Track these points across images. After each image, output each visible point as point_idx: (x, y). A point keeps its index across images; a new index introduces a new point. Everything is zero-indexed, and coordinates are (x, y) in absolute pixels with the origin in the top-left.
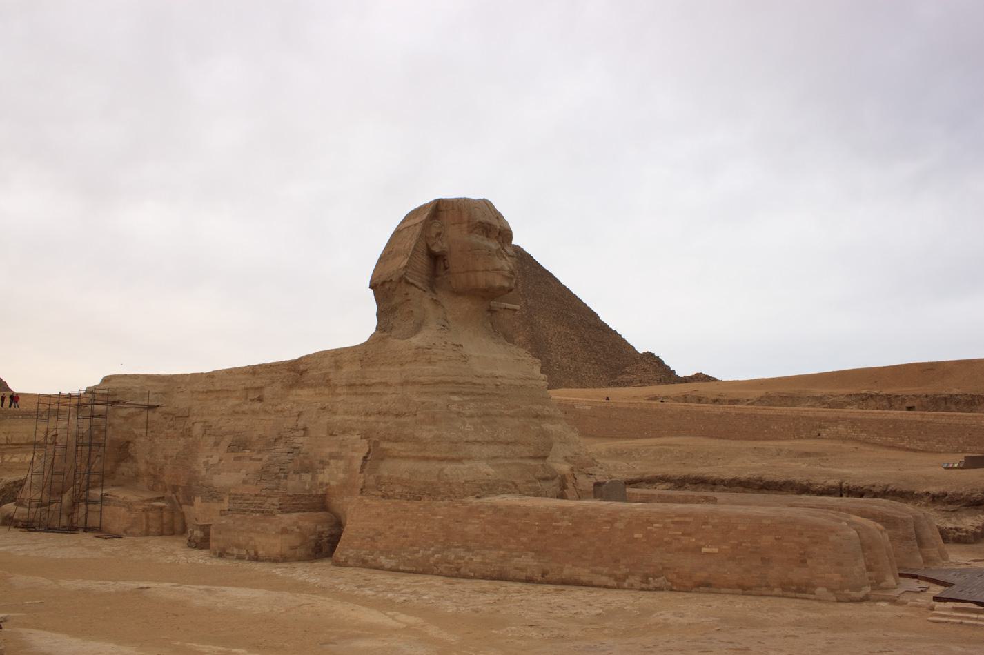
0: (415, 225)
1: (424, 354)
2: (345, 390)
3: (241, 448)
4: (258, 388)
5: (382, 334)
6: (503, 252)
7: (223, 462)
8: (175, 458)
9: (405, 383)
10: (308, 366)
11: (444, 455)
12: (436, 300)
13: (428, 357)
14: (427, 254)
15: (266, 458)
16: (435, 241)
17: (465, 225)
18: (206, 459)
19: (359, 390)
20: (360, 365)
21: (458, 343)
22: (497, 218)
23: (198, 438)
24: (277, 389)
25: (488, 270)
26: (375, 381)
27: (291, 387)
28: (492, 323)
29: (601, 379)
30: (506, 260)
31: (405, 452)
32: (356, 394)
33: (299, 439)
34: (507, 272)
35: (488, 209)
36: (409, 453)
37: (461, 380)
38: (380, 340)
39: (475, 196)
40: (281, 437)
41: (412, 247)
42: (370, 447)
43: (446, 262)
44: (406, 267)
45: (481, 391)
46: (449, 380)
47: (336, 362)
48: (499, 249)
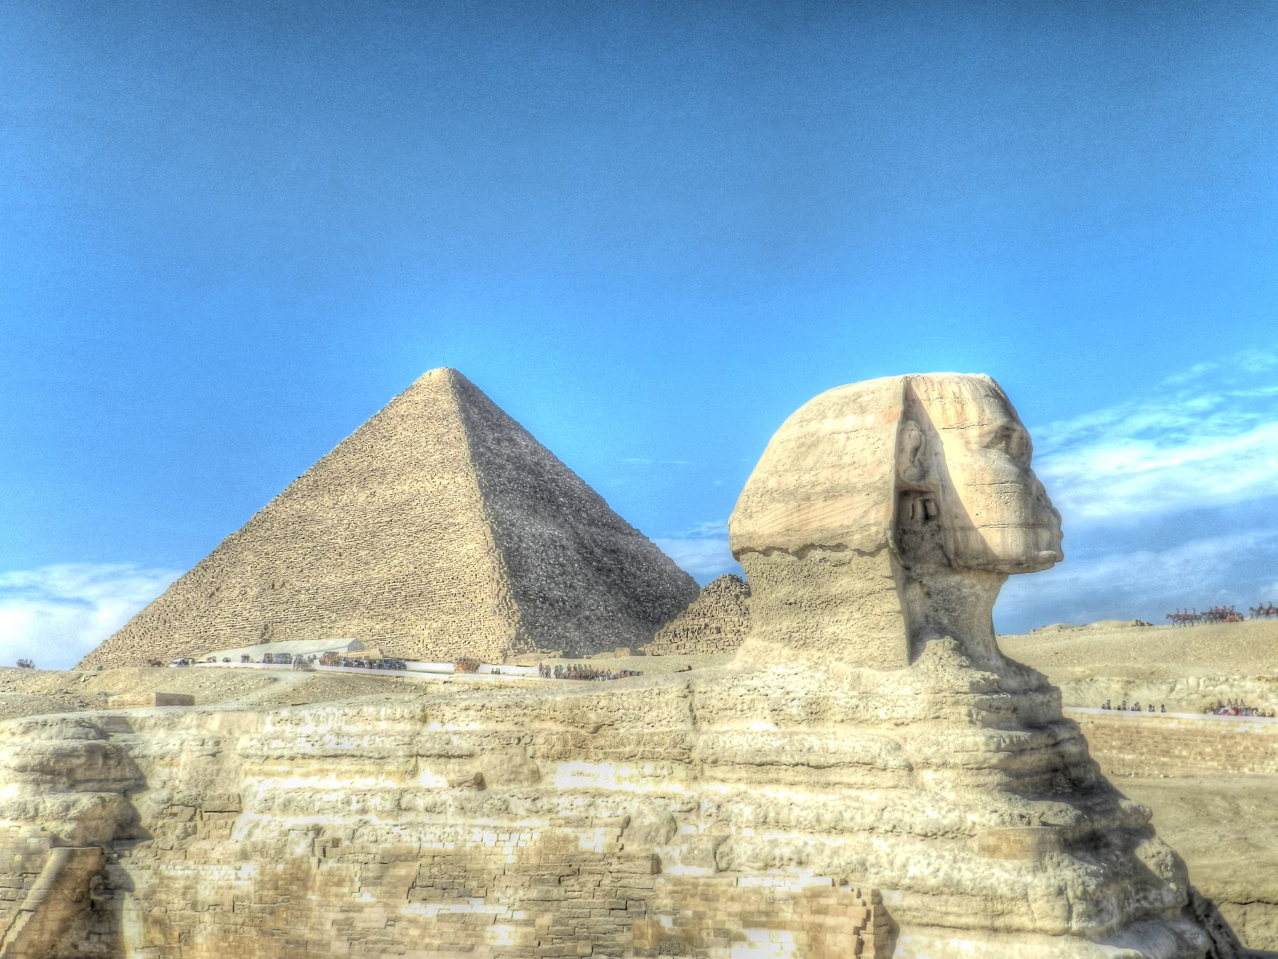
3: (455, 893)
4: (460, 757)
7: (399, 926)
8: (228, 906)
11: (1059, 925)
15: (546, 920)
18: (342, 916)
19: (789, 775)
23: (304, 866)
24: (518, 760)
29: (619, 620)
31: (960, 916)
32: (777, 781)
33: (638, 881)
36: (970, 920)
40: (578, 872)
42: (864, 904)
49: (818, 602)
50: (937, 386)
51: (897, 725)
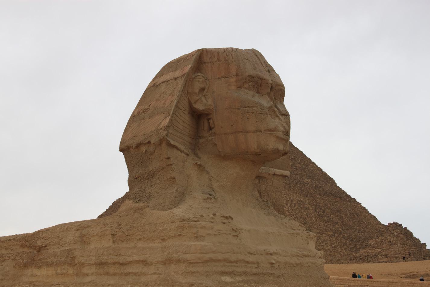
0: (176, 79)
1: (191, 227)
2: (94, 270)
5: (137, 205)
6: (276, 109)
9: (168, 262)
10: (48, 241)
12: (200, 166)
13: (195, 230)
14: (189, 113)
16: (198, 98)
17: (233, 80)
19: (111, 270)
20: (112, 240)
21: (228, 215)
22: (269, 71)
25: (260, 131)
26: (129, 259)
27: (25, 266)
28: (259, 192)
29: (339, 253)
30: (279, 119)
34: (281, 133)
35: (258, 62)
37: (233, 258)
38: (135, 211)
39: (243, 46)
41: (175, 103)
43: (211, 121)
44: (168, 126)
45: (255, 271)
46: (220, 258)
47: (82, 236)
48: (272, 107)
49: (146, 176)
50: (216, 54)
51: (162, 240)
